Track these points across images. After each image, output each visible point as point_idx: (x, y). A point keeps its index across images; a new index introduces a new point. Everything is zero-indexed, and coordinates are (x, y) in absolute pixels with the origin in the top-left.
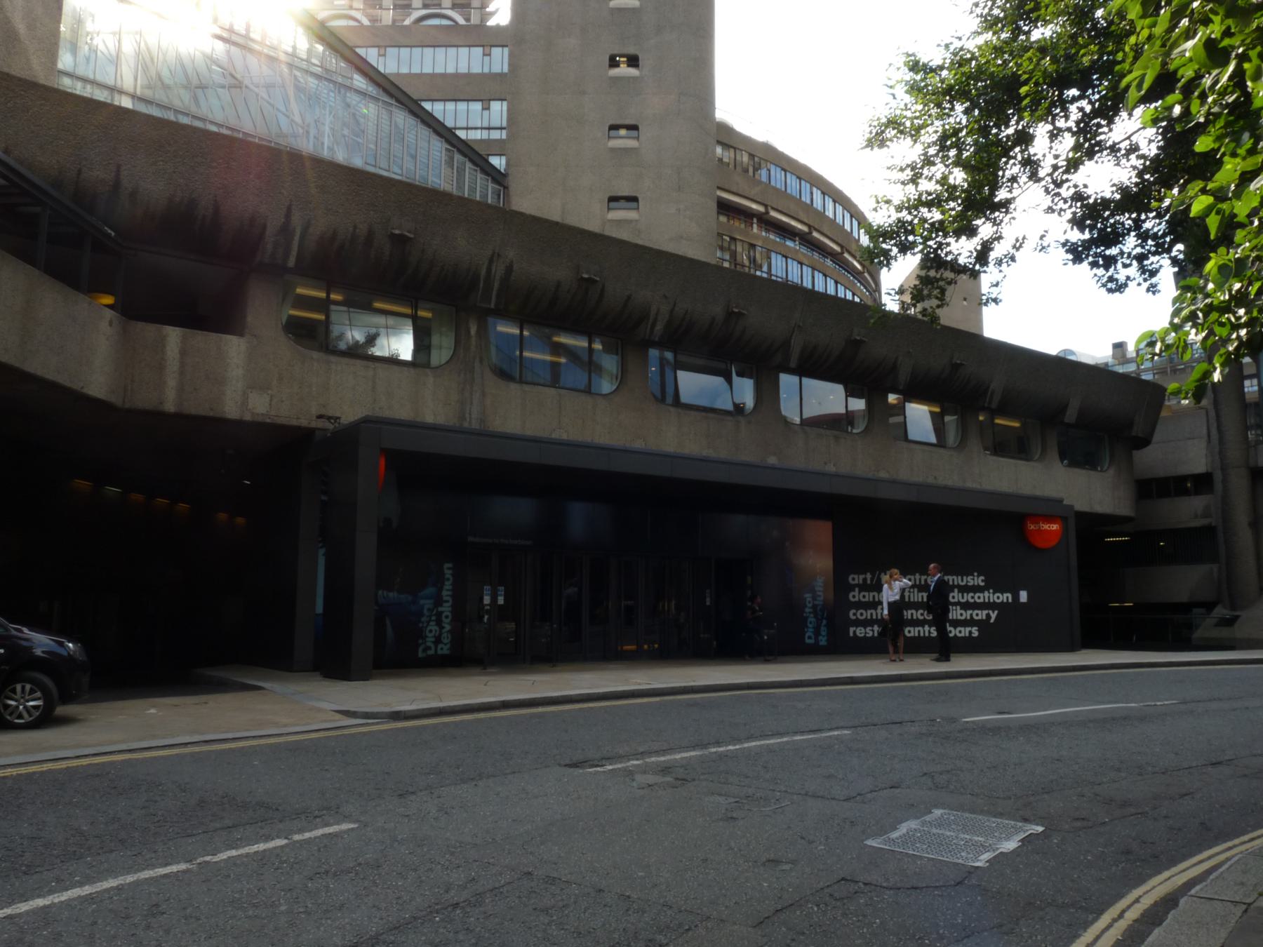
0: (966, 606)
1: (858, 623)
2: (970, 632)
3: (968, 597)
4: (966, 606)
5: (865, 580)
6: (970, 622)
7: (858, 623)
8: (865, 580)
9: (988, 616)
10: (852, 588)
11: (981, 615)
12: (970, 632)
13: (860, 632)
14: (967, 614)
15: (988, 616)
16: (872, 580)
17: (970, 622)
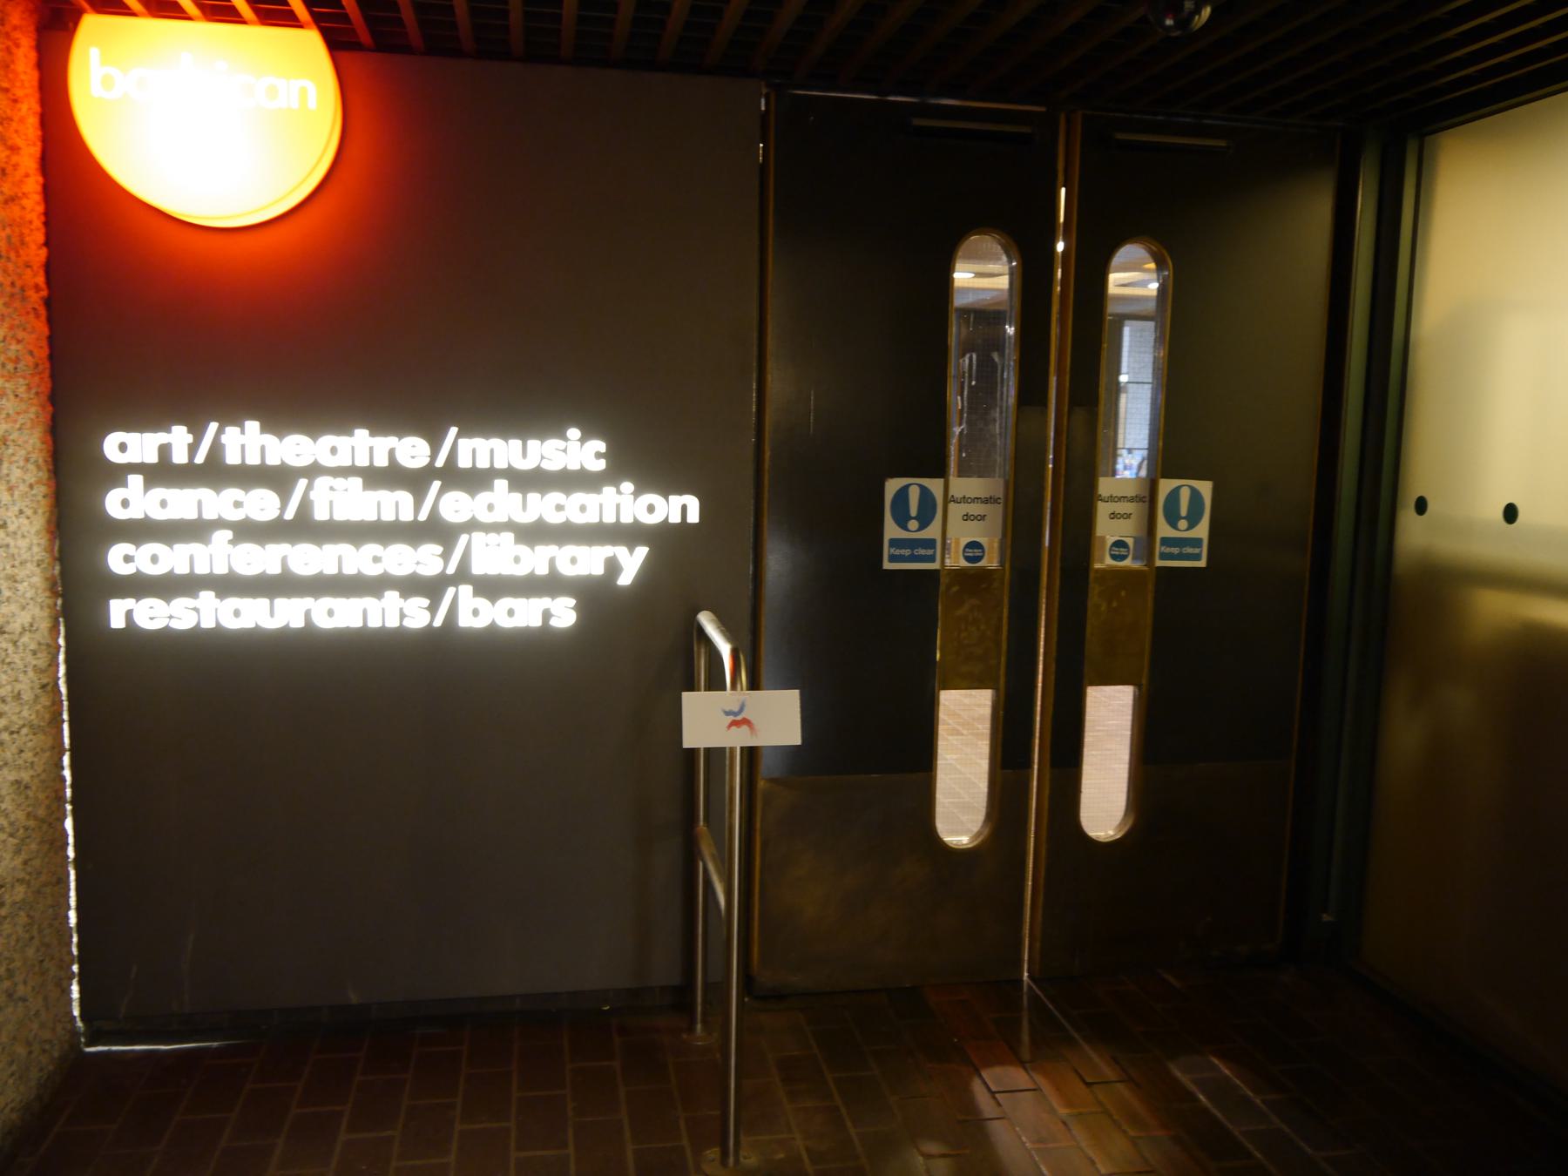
0: (534, 534)
1: (139, 586)
2: (547, 615)
3: (545, 507)
4: (534, 534)
5: (165, 450)
6: (550, 585)
7: (139, 586)
8: (165, 450)
9: (613, 567)
10: (118, 474)
11: (588, 561)
12: (547, 615)
13: (151, 615)
14: (536, 560)
15: (613, 567)
16: (193, 449)
17: (550, 585)
